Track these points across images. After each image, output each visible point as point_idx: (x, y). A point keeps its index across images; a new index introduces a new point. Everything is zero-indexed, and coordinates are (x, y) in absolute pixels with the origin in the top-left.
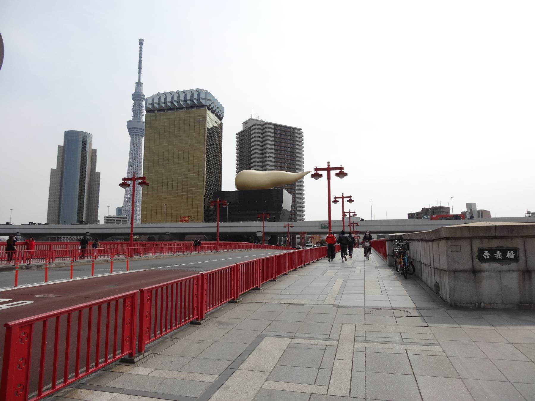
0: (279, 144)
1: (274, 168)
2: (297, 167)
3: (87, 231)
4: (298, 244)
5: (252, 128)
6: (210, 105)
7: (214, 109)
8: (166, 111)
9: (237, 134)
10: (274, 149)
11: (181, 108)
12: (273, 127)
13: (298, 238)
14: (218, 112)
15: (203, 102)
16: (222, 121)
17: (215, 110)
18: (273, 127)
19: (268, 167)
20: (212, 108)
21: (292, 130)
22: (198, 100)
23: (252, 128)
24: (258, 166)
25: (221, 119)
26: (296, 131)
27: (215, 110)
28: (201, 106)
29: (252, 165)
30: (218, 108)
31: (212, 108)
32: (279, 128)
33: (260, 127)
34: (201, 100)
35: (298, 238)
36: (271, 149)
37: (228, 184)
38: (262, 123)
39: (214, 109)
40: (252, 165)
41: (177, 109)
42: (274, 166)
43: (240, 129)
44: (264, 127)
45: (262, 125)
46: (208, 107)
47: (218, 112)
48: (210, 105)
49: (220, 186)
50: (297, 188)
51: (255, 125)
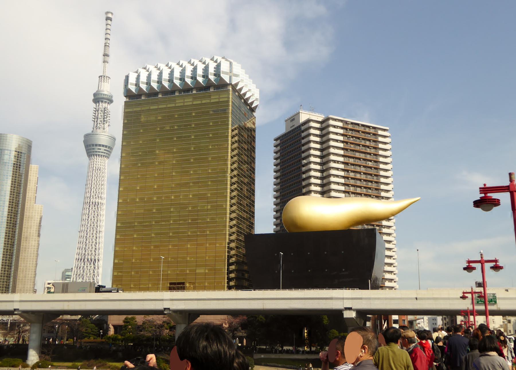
0: (350, 154)
1: (342, 195)
2: (383, 194)
3: (16, 306)
5: (303, 128)
6: (237, 84)
7: (242, 92)
8: (160, 96)
9: (276, 140)
10: (343, 163)
11: (186, 90)
12: (340, 124)
13: (396, 322)
15: (226, 78)
16: (254, 114)
17: (245, 94)
18: (340, 124)
19: (333, 194)
20: (241, 89)
21: (372, 131)
22: (217, 74)
23: (303, 128)
24: (316, 192)
25: (253, 110)
26: (380, 132)
27: (245, 94)
28: (221, 85)
29: (304, 191)
30: (249, 90)
31: (241, 89)
32: (350, 126)
33: (318, 125)
34: (222, 75)
35: (396, 322)
36: (338, 162)
37: (265, 224)
38: (320, 119)
39: (242, 92)
40: (304, 191)
41: (180, 91)
42: (344, 192)
43: (282, 130)
44: (324, 125)
45: (321, 123)
46: (234, 87)
48: (237, 84)
49: (251, 226)
50: (385, 230)
51: (308, 121)
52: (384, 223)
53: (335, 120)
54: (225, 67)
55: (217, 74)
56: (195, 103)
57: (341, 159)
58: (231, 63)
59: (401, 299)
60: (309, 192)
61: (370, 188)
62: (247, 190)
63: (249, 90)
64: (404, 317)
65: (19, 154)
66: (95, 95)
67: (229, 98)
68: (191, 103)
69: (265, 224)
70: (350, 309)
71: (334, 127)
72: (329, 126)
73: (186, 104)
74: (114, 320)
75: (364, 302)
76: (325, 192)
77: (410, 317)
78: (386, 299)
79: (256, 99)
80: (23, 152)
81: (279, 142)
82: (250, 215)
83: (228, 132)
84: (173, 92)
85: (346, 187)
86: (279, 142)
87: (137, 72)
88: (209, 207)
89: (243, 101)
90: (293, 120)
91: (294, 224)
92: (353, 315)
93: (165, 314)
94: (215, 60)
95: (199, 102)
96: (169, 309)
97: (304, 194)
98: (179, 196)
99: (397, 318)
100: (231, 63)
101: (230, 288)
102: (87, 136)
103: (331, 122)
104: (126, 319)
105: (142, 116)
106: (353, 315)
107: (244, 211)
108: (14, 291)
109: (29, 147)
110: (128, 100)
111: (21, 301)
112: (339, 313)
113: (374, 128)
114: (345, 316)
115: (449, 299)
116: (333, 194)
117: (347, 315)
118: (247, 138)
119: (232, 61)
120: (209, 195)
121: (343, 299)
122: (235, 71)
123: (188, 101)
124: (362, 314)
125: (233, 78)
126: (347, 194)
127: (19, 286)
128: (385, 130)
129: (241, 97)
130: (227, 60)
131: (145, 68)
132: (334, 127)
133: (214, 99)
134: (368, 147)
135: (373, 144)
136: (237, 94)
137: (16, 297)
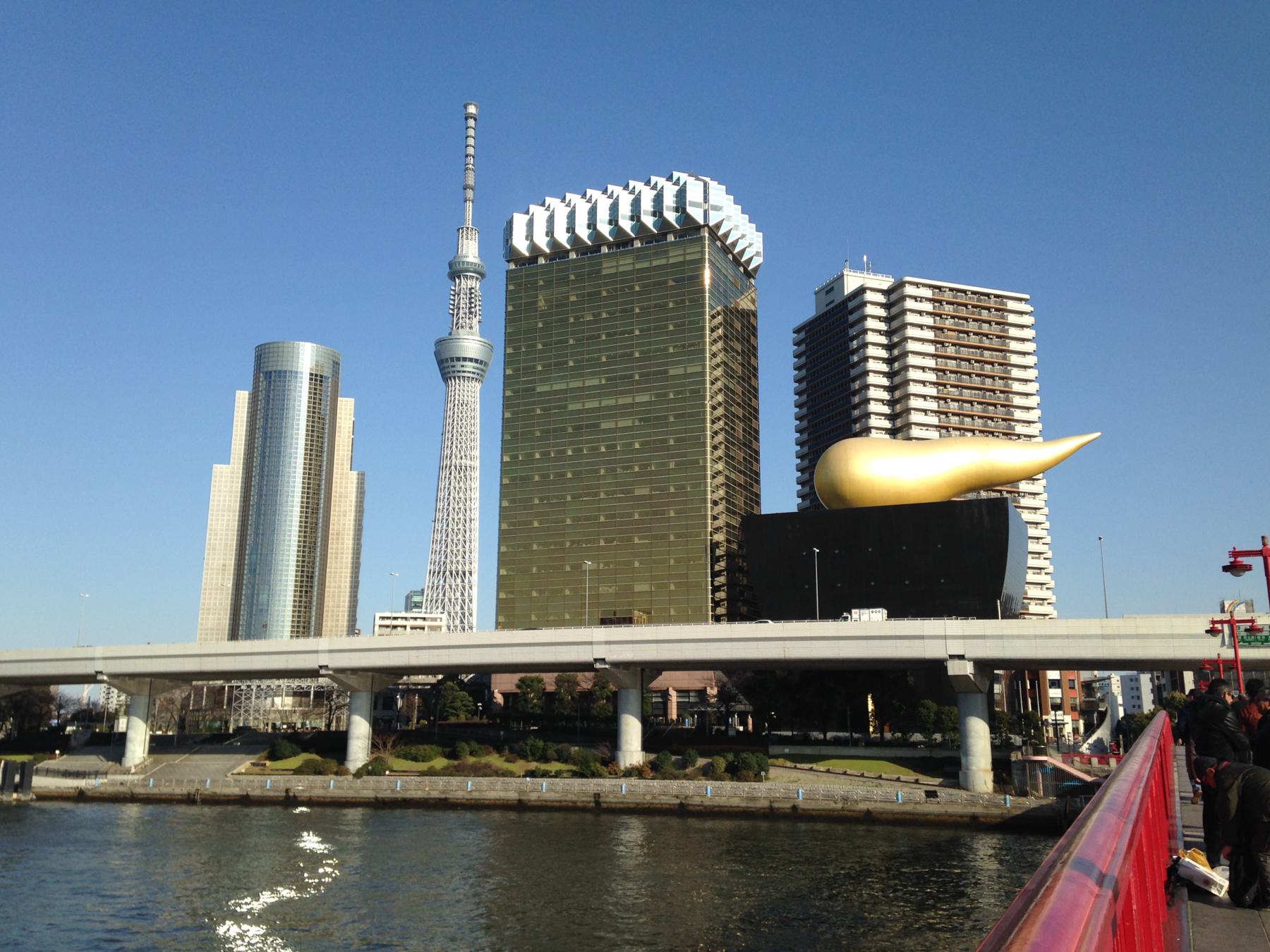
1: (934, 434)
2: (1019, 429)
3: (323, 660)
4: (1057, 707)
5: (851, 305)
6: (718, 226)
7: (729, 242)
9: (797, 331)
12: (928, 293)
13: (1055, 684)
14: (743, 252)
15: (697, 214)
17: (734, 244)
18: (928, 293)
20: (726, 235)
22: (680, 207)
23: (851, 305)
26: (1011, 305)
27: (734, 244)
28: (690, 228)
30: (743, 236)
31: (726, 235)
32: (948, 296)
34: (690, 210)
35: (1055, 684)
38: (885, 286)
39: (729, 242)
41: (610, 245)
43: (808, 311)
44: (894, 297)
45: (886, 293)
46: (713, 231)
47: (743, 252)
48: (718, 226)
49: (755, 499)
51: (862, 290)
52: (1024, 486)
53: (917, 285)
54: (694, 191)
55: (680, 207)
56: (638, 266)
57: (931, 363)
58: (705, 184)
59: (1067, 637)
60: (866, 431)
61: (992, 419)
62: (744, 430)
63: (743, 236)
64: (1072, 675)
65: (316, 379)
66: (450, 265)
67: (703, 252)
68: (630, 268)
69: (780, 495)
70: (961, 657)
71: (915, 298)
72: (903, 298)
73: (621, 269)
74: (501, 686)
75: (989, 643)
76: (899, 429)
77: (1085, 675)
78: (1036, 637)
79: (758, 254)
80: (325, 374)
81: (803, 335)
82: (751, 478)
83: (704, 320)
84: (596, 248)
85: (943, 417)
86: (803, 335)
87: (527, 213)
88: (672, 466)
89: (730, 257)
90: (832, 289)
91: (836, 494)
92: (968, 669)
93: (596, 670)
94: (675, 179)
95: (646, 265)
96: (603, 660)
97: (856, 435)
98: (615, 446)
99: (1058, 677)
100: (705, 184)
101: (717, 619)
102: (440, 343)
103: (909, 290)
104: (522, 680)
105: (540, 297)
106: (968, 669)
107: (740, 472)
108: (319, 633)
109: (336, 364)
110: (512, 266)
111: (331, 651)
112: (937, 666)
113: (997, 296)
114: (950, 672)
115: (1172, 636)
116: (915, 432)
117: (954, 668)
118: (742, 331)
119: (708, 179)
120: (672, 442)
121: (945, 637)
122: (713, 200)
123: (626, 264)
124: (985, 666)
125: (712, 213)
126: (944, 431)
127: (328, 623)
128: (1021, 300)
129: (727, 250)
130: (698, 179)
131: (543, 204)
132: (915, 298)
133: (675, 257)
134: (986, 335)
135: (996, 329)
136: (718, 243)
137: (322, 643)
